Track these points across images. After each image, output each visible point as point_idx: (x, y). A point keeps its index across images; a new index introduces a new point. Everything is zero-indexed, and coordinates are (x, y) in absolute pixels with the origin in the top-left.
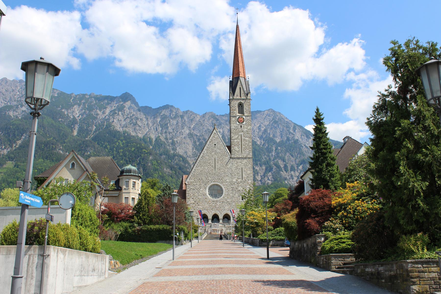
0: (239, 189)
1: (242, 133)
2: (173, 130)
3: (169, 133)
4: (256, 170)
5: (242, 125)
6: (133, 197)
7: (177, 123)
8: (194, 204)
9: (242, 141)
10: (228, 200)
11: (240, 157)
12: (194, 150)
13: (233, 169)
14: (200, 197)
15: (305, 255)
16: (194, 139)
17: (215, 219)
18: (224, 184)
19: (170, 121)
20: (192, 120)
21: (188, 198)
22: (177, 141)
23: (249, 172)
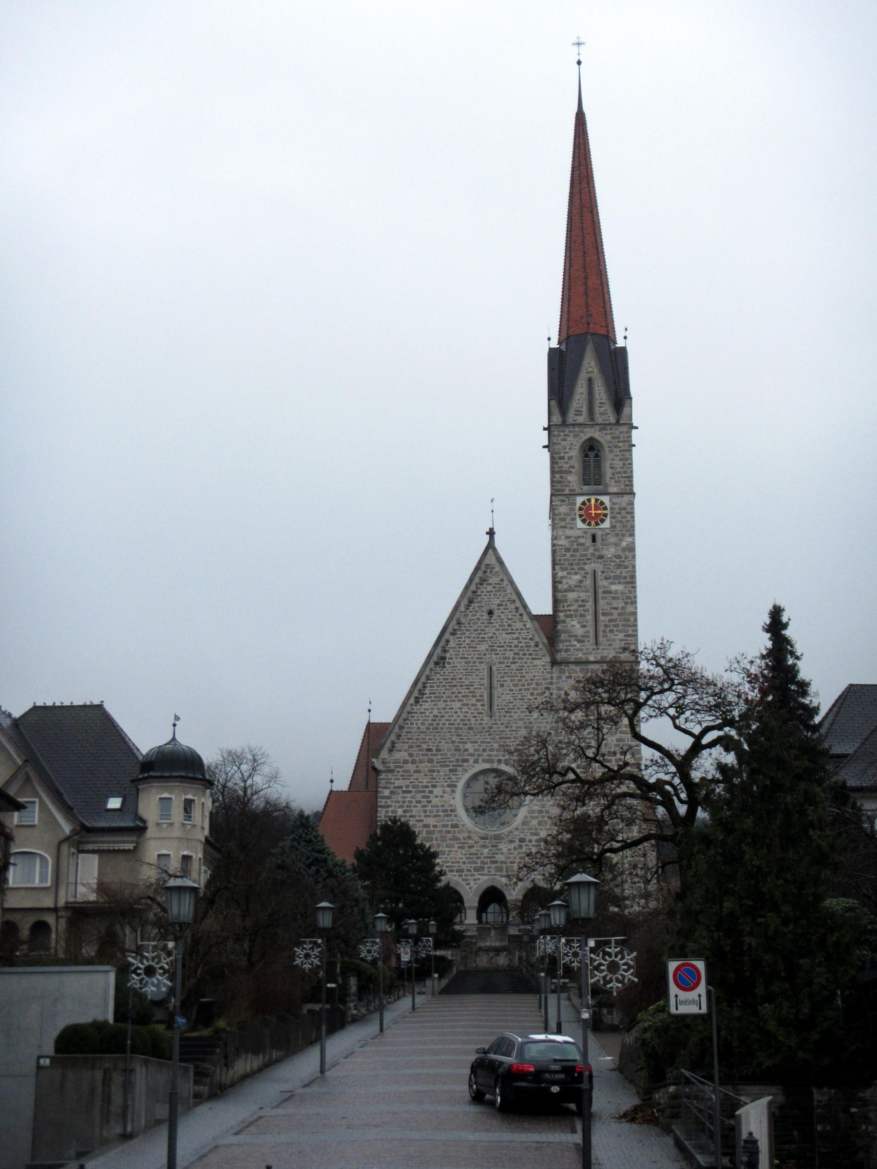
5: (599, 534)
9: (600, 595)
11: (592, 658)
14: (431, 821)
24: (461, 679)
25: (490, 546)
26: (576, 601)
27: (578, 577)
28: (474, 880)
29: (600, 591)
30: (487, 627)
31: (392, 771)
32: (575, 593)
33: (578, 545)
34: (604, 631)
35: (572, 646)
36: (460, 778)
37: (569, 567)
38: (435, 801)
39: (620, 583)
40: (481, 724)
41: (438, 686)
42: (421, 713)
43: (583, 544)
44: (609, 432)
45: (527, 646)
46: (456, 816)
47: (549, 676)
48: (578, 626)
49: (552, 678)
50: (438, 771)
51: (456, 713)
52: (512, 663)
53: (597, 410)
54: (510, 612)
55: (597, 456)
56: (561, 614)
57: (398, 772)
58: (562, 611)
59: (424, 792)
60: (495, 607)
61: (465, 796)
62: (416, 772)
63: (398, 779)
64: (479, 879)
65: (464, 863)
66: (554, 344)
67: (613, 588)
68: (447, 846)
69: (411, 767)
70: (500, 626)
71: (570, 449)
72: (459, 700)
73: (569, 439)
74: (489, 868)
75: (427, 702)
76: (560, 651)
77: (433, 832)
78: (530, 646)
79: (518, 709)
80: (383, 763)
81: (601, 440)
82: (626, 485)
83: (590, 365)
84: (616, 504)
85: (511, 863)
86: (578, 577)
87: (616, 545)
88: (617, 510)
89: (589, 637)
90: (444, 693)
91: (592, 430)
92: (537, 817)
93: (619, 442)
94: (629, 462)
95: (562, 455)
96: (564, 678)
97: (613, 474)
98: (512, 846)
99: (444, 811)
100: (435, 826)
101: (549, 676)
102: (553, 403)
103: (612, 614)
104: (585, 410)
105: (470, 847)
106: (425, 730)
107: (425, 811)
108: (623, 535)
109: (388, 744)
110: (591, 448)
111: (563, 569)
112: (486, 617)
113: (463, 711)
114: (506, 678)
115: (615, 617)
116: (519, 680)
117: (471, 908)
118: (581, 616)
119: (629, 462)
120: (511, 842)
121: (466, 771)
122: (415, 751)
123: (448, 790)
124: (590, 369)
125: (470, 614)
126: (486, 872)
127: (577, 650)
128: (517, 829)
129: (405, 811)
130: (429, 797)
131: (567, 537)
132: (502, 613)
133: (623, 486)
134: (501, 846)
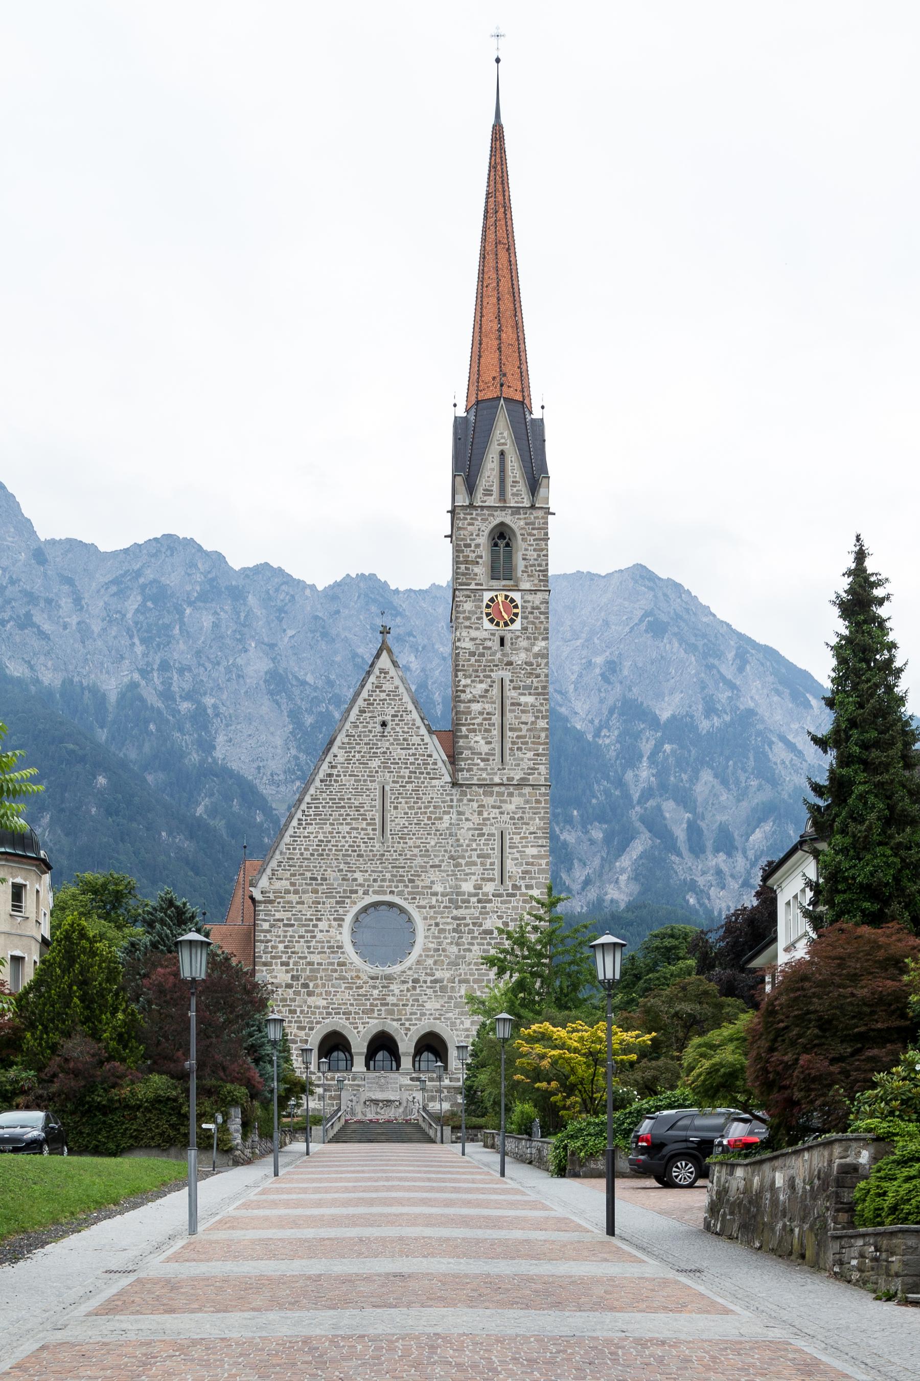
0: (488, 924)
1: (507, 675)
2: (198, 654)
3: (181, 671)
4: (565, 844)
5: (508, 637)
6: (18, 953)
7: (216, 625)
8: (289, 986)
9: (508, 707)
10: (438, 975)
11: (497, 780)
12: (293, 751)
13: (464, 835)
14: (316, 958)
15: (780, 1226)
16: (290, 698)
17: (380, 1056)
18: (422, 903)
19: (181, 613)
20: (281, 610)
21: (265, 964)
22: (215, 707)
23: (534, 851)
24: (350, 799)
26: (481, 713)
27: (484, 686)
28: (363, 1023)
29: (508, 702)
30: (381, 740)
31: (271, 902)
32: (479, 704)
33: (484, 648)
34: (511, 749)
35: (475, 765)
36: (348, 911)
37: (474, 674)
38: (319, 936)
39: (530, 694)
40: (371, 851)
41: (324, 807)
42: (304, 837)
43: (490, 648)
44: (522, 516)
45: (424, 764)
46: (343, 953)
47: (448, 798)
48: (482, 742)
49: (452, 801)
50: (324, 903)
51: (344, 837)
52: (407, 783)
53: (509, 491)
54: (405, 724)
55: (508, 545)
56: (464, 729)
57: (279, 903)
58: (464, 725)
59: (308, 925)
60: (389, 718)
61: (353, 932)
62: (298, 903)
63: (279, 911)
64: (368, 1023)
65: (352, 1005)
66: (461, 413)
67: (523, 699)
68: (333, 986)
69: (294, 898)
70: (395, 740)
71: (478, 535)
72: (347, 824)
73: (476, 523)
74: (378, 1010)
75: (312, 824)
76: (462, 770)
77: (318, 970)
78: (428, 764)
79: (414, 834)
80: (262, 892)
81: (513, 526)
82: (541, 581)
83: (502, 434)
84: (529, 602)
85: (403, 1005)
86: (484, 686)
87: (527, 650)
88: (529, 609)
89: (494, 755)
90: (331, 815)
91: (504, 513)
92: (433, 956)
93: (533, 529)
94: (544, 553)
95: (469, 542)
96: (465, 802)
97: (526, 567)
98: (405, 987)
99: (329, 948)
100: (320, 964)
101: (448, 798)
102: (459, 479)
103: (521, 730)
104: (495, 489)
105: (357, 988)
106: (309, 856)
107: (309, 947)
108: (536, 639)
109: (269, 871)
110: (502, 536)
111: (466, 677)
112: (379, 728)
113: (352, 835)
114: (400, 800)
115: (523, 733)
116: (414, 803)
117: (359, 1054)
118: (486, 730)
119: (544, 553)
120: (404, 982)
121: (355, 903)
123: (335, 924)
124: (503, 441)
125: (360, 725)
126: (376, 1015)
127: (482, 769)
128: (410, 969)
129: (286, 947)
130: (313, 931)
131: (472, 639)
132: (397, 725)
133: (536, 582)
134: (392, 987)
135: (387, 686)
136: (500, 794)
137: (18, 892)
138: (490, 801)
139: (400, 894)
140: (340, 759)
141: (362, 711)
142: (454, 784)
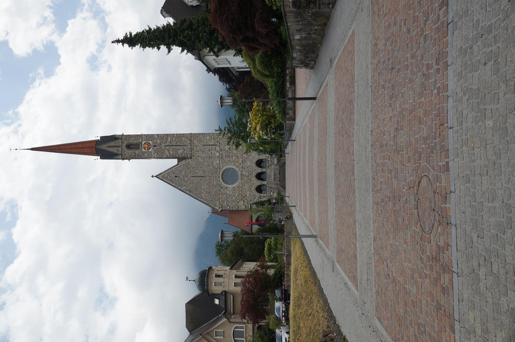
0: (227, 149)
1: (163, 145)
6: (234, 276)
8: (244, 201)
10: (241, 162)
13: (204, 155)
14: (237, 194)
15: (313, 35)
17: (262, 177)
25: (156, 176)
67: (169, 140)
69: (221, 200)
110: (129, 147)
112: (177, 178)
122: (216, 199)
135: (166, 176)
136: (193, 146)
137: (218, 276)
138: (195, 149)
139: (219, 172)
140: (185, 188)
141: (173, 182)
142: (191, 158)
